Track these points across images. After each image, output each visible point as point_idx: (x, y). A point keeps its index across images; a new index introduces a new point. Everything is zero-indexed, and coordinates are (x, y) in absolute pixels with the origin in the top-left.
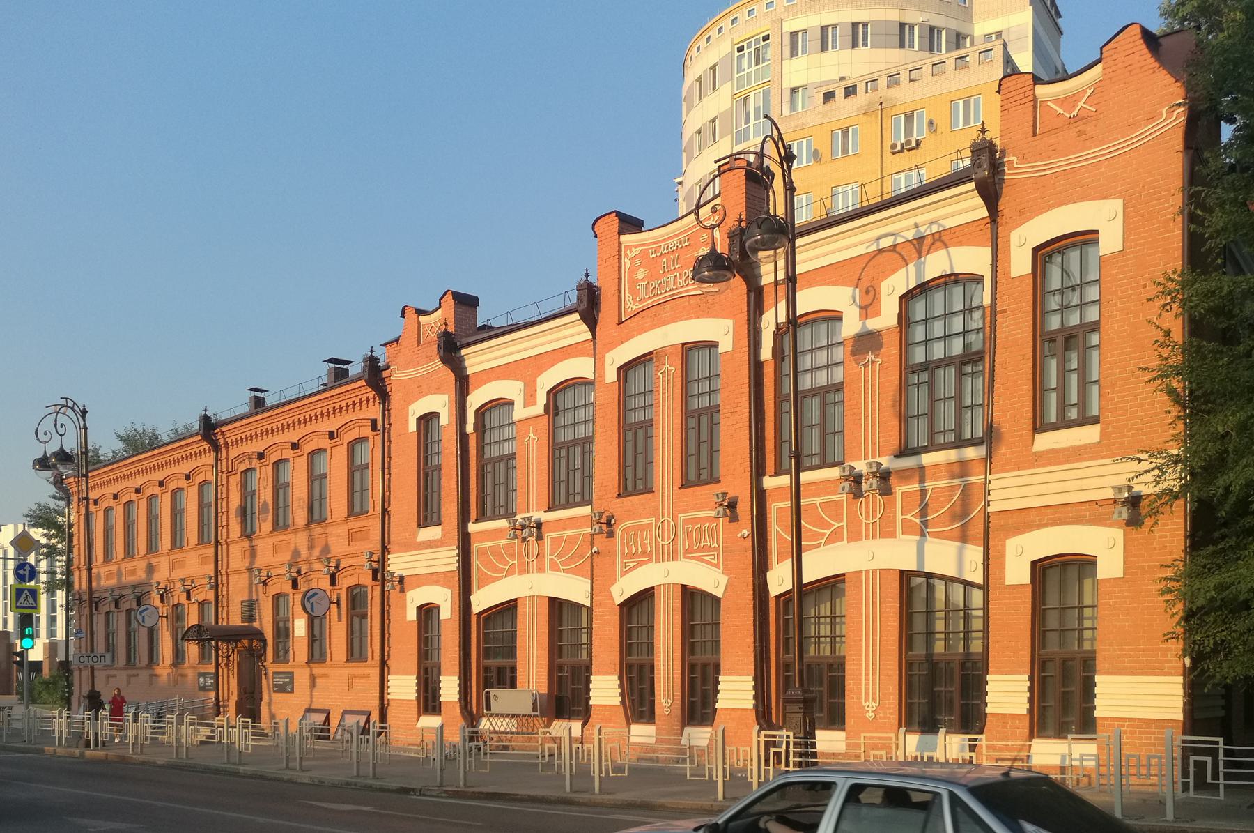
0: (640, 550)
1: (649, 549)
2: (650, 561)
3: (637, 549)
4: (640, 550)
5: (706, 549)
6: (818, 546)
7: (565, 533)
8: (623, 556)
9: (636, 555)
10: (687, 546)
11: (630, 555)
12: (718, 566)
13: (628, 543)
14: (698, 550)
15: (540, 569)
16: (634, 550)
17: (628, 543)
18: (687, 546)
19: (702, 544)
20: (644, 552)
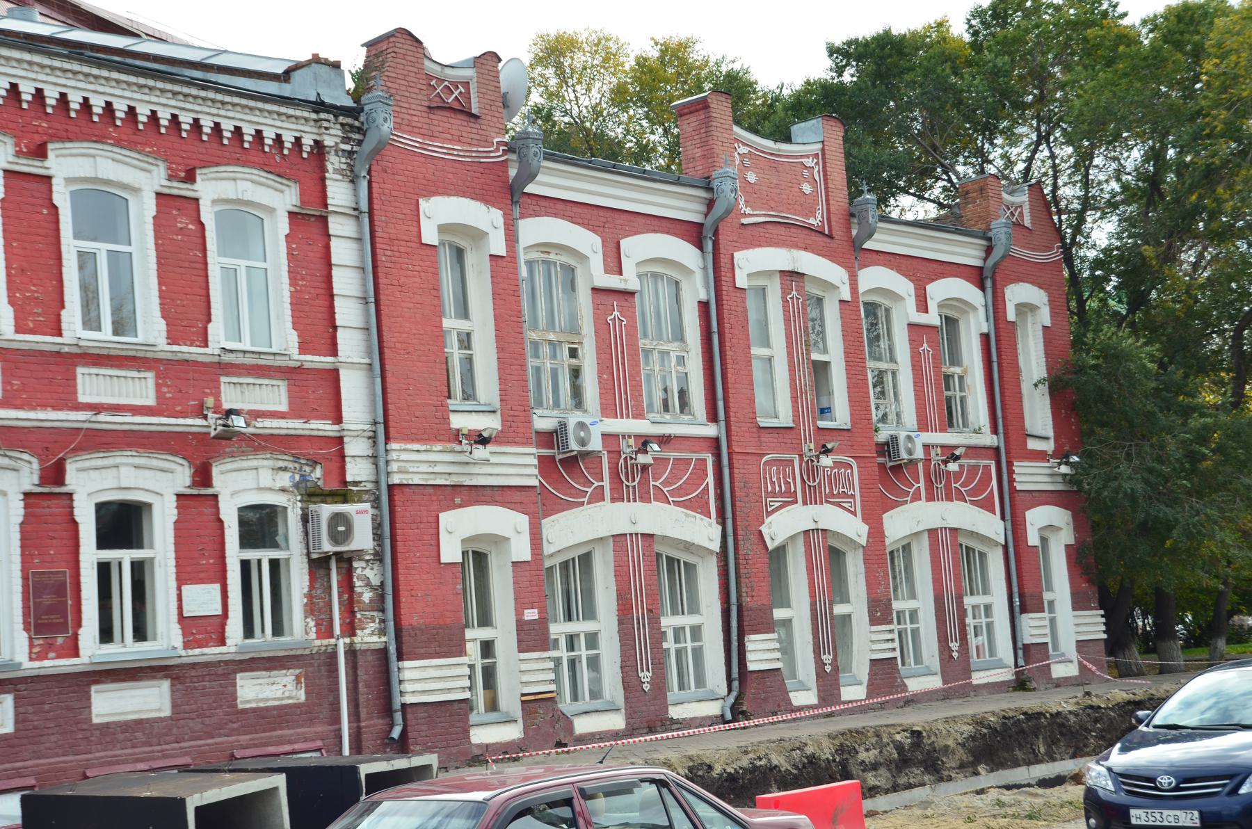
0: (783, 489)
1: (793, 489)
2: (796, 502)
3: (780, 486)
4: (783, 489)
5: (845, 495)
6: (906, 502)
7: (673, 455)
8: (766, 491)
9: (781, 494)
10: (827, 491)
11: (773, 494)
12: (854, 513)
13: (771, 479)
14: (839, 495)
15: (645, 498)
16: (777, 489)
17: (771, 479)
18: (827, 491)
19: (841, 490)
20: (788, 493)
